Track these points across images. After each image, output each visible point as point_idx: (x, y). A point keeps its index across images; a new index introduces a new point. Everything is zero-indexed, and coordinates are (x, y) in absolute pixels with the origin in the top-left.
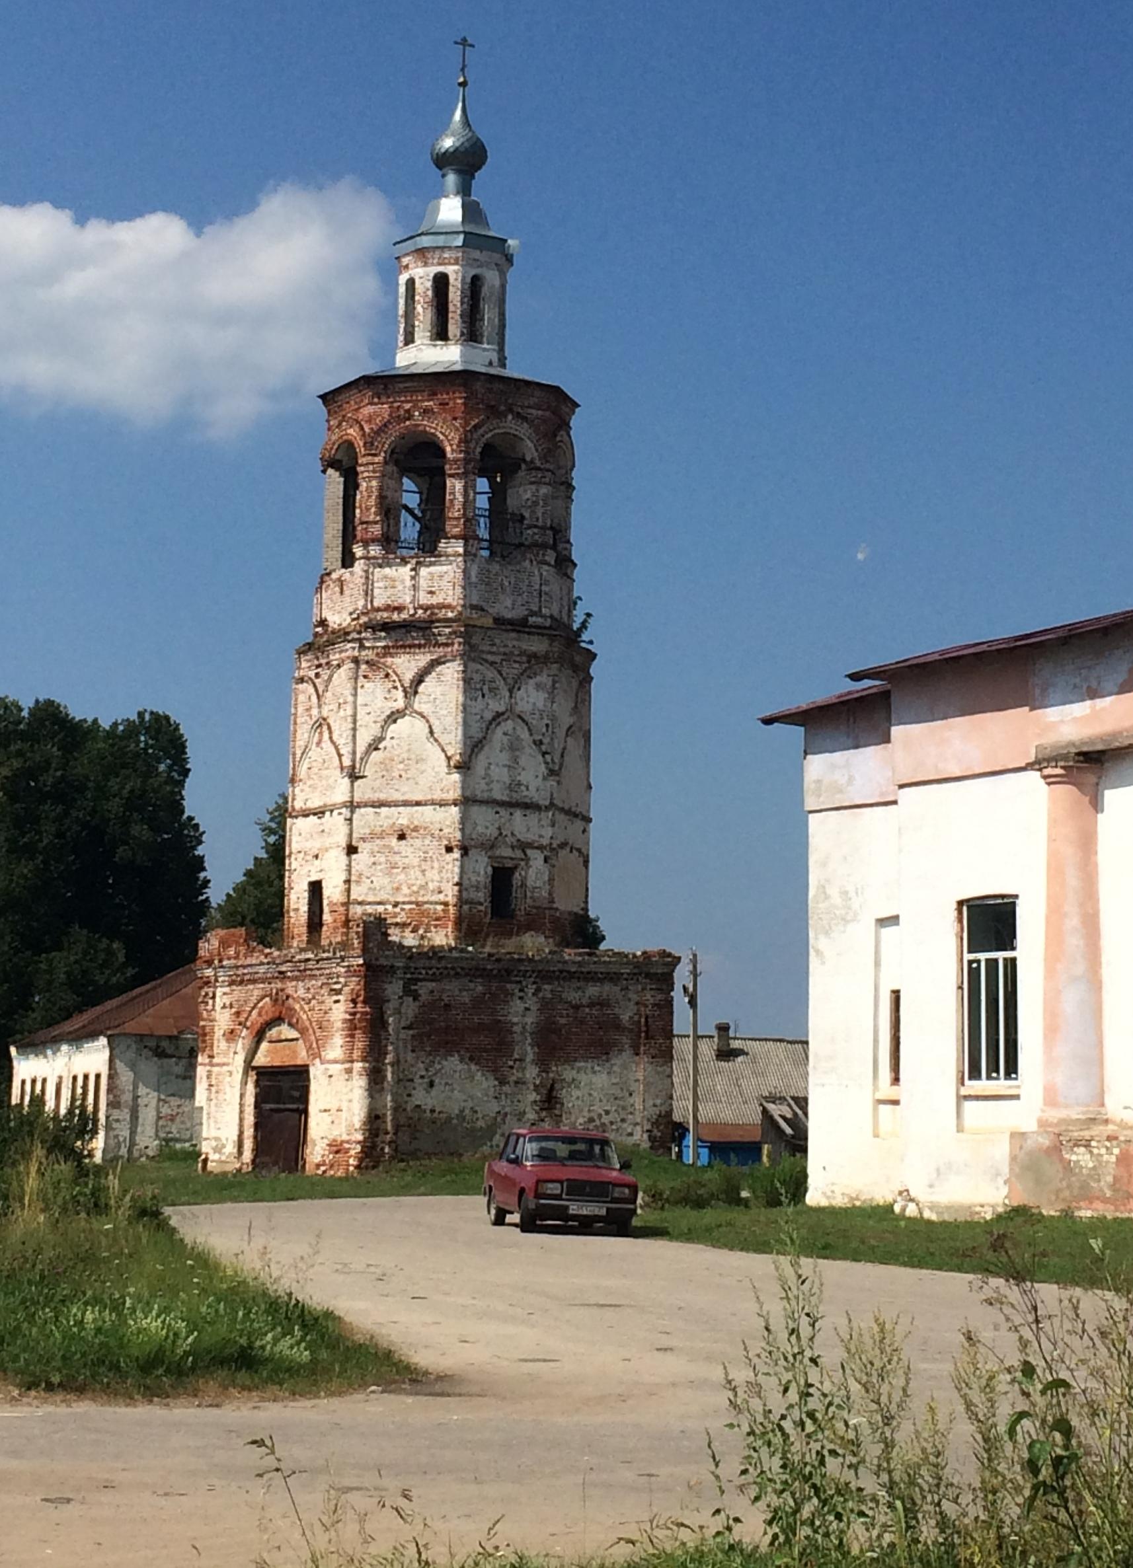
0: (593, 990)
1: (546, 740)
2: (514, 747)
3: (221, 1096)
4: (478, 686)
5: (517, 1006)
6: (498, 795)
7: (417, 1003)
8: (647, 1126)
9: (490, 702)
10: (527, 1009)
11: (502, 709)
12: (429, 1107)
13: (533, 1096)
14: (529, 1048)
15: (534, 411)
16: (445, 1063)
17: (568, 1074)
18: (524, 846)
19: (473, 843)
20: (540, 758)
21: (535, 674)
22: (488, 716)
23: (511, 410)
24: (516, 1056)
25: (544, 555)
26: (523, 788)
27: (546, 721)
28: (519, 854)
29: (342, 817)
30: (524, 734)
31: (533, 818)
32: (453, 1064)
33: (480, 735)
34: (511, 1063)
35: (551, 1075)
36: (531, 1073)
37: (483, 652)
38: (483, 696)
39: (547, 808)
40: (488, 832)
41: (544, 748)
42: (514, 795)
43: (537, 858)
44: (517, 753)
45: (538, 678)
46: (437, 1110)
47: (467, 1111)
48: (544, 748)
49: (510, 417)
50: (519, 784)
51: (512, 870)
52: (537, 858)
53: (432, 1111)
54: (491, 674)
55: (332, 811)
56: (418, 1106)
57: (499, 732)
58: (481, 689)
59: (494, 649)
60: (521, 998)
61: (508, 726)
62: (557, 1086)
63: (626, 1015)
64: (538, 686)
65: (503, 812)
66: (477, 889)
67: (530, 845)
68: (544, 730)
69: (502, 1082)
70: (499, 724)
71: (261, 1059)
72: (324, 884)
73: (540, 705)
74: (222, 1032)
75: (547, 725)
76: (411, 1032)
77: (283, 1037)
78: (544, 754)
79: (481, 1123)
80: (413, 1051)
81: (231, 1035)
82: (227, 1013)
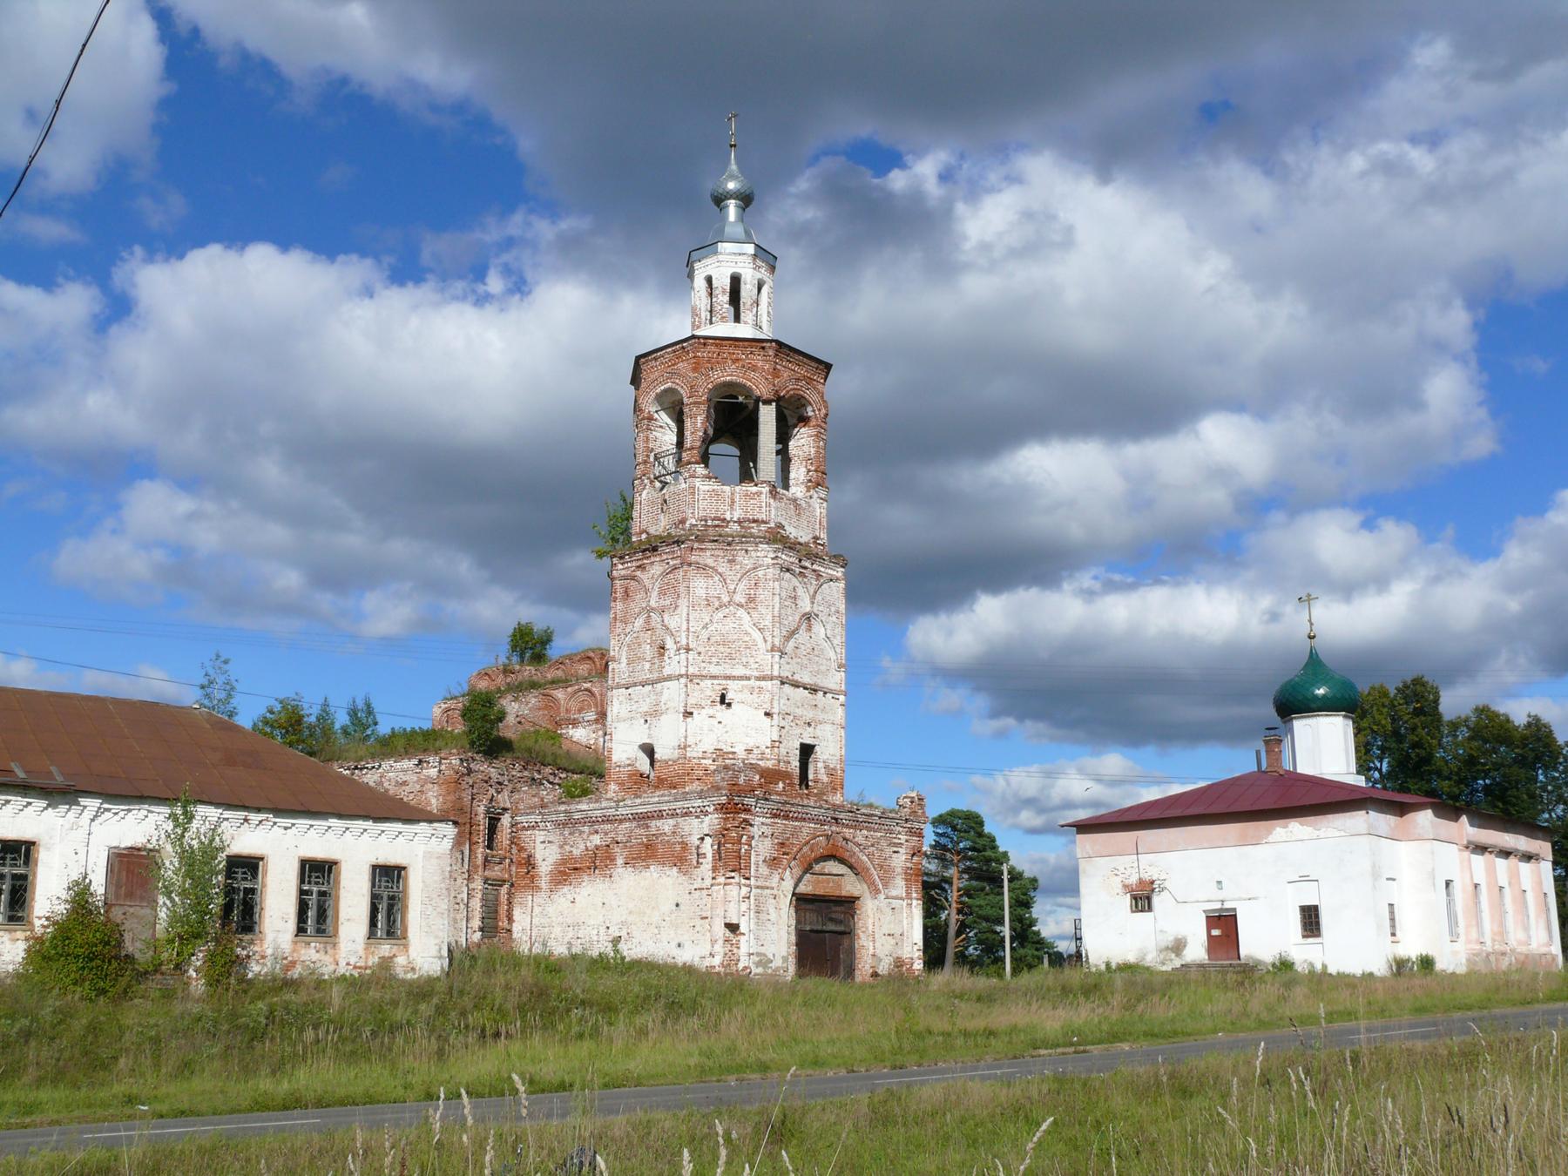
3: (763, 916)
29: (838, 702)
55: (825, 693)
71: (802, 889)
72: (817, 748)
74: (761, 858)
77: (827, 871)
81: (773, 863)
82: (768, 842)
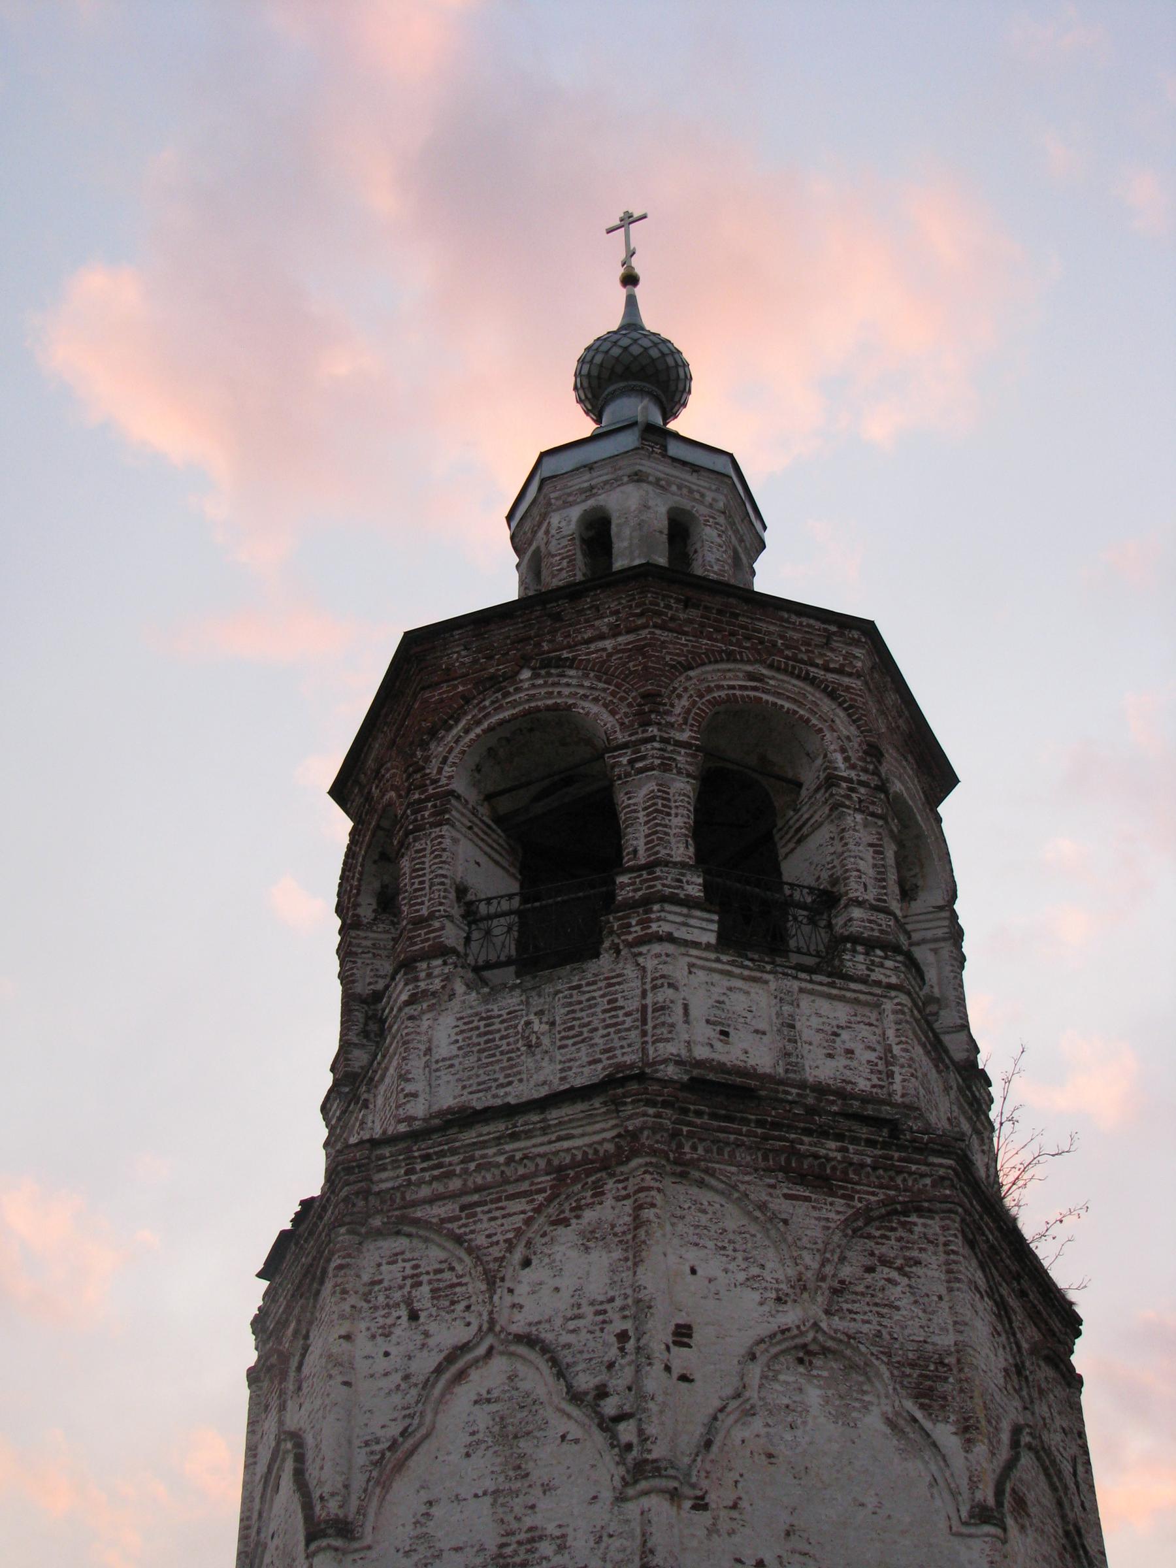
1: (619, 1381)
4: (397, 1296)
9: (432, 1327)
11: (459, 1334)
15: (608, 644)
20: (599, 1438)
21: (578, 1209)
22: (425, 1363)
23: (524, 661)
25: (645, 923)
26: (546, 1548)
27: (619, 1326)
33: (395, 1430)
37: (414, 1204)
38: (414, 1316)
41: (610, 1407)
44: (524, 1445)
45: (589, 1215)
48: (610, 1407)
50: (535, 1537)
54: (433, 1255)
57: (465, 1394)
58: (409, 1302)
59: (455, 1184)
64: (590, 1238)
68: (614, 1352)
70: (461, 1376)
73: (597, 1288)
75: (623, 1336)
78: (608, 1425)
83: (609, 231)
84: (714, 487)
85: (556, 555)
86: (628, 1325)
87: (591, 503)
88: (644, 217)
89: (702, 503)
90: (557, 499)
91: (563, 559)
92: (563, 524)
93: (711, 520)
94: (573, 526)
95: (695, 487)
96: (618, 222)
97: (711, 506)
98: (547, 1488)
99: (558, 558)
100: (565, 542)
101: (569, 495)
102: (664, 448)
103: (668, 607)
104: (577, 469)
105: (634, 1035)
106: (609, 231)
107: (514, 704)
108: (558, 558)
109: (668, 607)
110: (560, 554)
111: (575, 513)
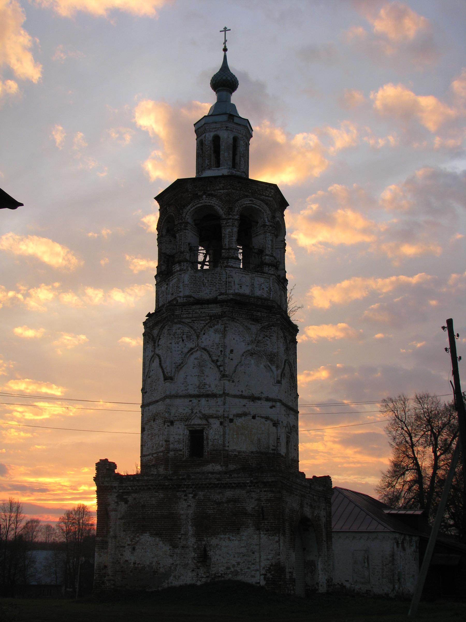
0: (229, 494)
1: (220, 359)
2: (201, 365)
4: (180, 336)
5: (183, 504)
6: (191, 392)
7: (127, 506)
8: (263, 572)
9: (187, 343)
10: (189, 506)
11: (193, 346)
12: (133, 561)
13: (193, 554)
14: (190, 528)
15: (222, 191)
16: (142, 537)
17: (214, 541)
18: (206, 417)
19: (176, 418)
20: (217, 369)
21: (214, 325)
22: (186, 350)
23: (204, 193)
24: (182, 532)
25: (227, 263)
26: (207, 386)
27: (221, 349)
28: (204, 422)
30: (206, 356)
31: (212, 402)
32: (146, 538)
33: (180, 362)
34: (180, 536)
35: (204, 543)
36: (192, 541)
37: (183, 318)
38: (183, 340)
39: (220, 396)
40: (185, 412)
41: (219, 364)
42: (202, 391)
43: (215, 424)
44: (203, 368)
45: (216, 327)
46: (137, 562)
47: (154, 564)
48: (219, 364)
49: (204, 197)
50: (205, 384)
51: (202, 431)
52: (215, 424)
53: (134, 563)
54: (187, 329)
56: (127, 561)
57: (193, 357)
58: (182, 338)
59: (190, 316)
60: (185, 500)
61: (197, 354)
62: (208, 549)
63: (250, 506)
64: (216, 331)
65: (195, 401)
66: (179, 442)
67: (212, 417)
68: (219, 354)
69: (175, 547)
70: (192, 354)
73: (217, 340)
75: (221, 351)
76: (123, 521)
78: (218, 367)
79: (162, 570)
80: (124, 531)
83: (221, 31)
84: (243, 129)
85: (207, 146)
86: (222, 349)
87: (216, 133)
88: (230, 30)
89: (240, 133)
90: (208, 129)
91: (208, 147)
92: (209, 137)
93: (242, 139)
94: (211, 138)
95: (239, 129)
96: (223, 30)
97: (242, 134)
98: (207, 376)
99: (208, 146)
100: (209, 142)
101: (211, 128)
102: (233, 120)
103: (235, 183)
104: (213, 123)
105: (224, 286)
106: (221, 31)
107: (201, 203)
108: (208, 146)
109: (235, 183)
110: (208, 146)
111: (212, 134)
